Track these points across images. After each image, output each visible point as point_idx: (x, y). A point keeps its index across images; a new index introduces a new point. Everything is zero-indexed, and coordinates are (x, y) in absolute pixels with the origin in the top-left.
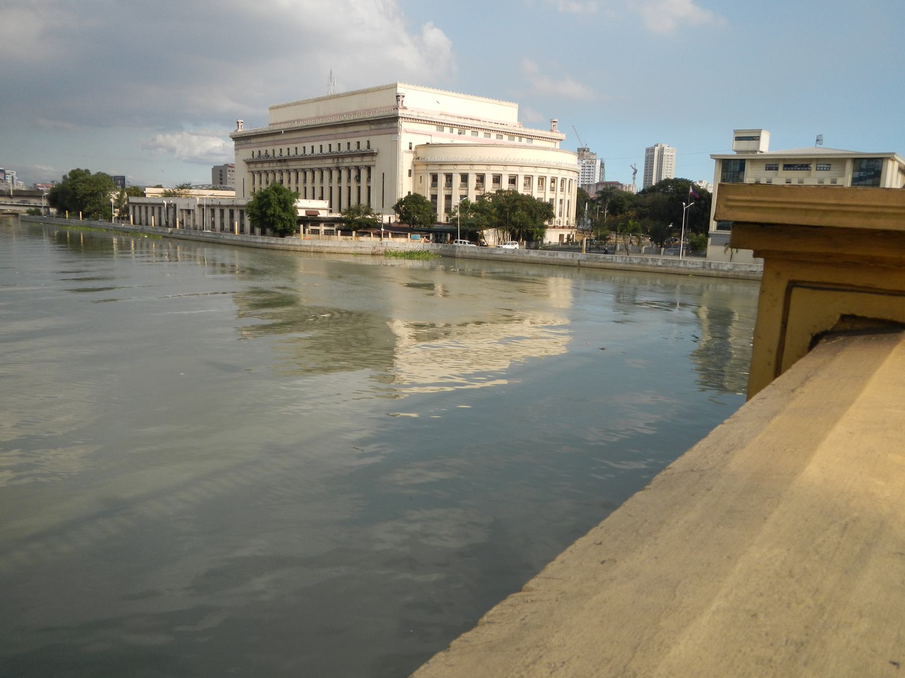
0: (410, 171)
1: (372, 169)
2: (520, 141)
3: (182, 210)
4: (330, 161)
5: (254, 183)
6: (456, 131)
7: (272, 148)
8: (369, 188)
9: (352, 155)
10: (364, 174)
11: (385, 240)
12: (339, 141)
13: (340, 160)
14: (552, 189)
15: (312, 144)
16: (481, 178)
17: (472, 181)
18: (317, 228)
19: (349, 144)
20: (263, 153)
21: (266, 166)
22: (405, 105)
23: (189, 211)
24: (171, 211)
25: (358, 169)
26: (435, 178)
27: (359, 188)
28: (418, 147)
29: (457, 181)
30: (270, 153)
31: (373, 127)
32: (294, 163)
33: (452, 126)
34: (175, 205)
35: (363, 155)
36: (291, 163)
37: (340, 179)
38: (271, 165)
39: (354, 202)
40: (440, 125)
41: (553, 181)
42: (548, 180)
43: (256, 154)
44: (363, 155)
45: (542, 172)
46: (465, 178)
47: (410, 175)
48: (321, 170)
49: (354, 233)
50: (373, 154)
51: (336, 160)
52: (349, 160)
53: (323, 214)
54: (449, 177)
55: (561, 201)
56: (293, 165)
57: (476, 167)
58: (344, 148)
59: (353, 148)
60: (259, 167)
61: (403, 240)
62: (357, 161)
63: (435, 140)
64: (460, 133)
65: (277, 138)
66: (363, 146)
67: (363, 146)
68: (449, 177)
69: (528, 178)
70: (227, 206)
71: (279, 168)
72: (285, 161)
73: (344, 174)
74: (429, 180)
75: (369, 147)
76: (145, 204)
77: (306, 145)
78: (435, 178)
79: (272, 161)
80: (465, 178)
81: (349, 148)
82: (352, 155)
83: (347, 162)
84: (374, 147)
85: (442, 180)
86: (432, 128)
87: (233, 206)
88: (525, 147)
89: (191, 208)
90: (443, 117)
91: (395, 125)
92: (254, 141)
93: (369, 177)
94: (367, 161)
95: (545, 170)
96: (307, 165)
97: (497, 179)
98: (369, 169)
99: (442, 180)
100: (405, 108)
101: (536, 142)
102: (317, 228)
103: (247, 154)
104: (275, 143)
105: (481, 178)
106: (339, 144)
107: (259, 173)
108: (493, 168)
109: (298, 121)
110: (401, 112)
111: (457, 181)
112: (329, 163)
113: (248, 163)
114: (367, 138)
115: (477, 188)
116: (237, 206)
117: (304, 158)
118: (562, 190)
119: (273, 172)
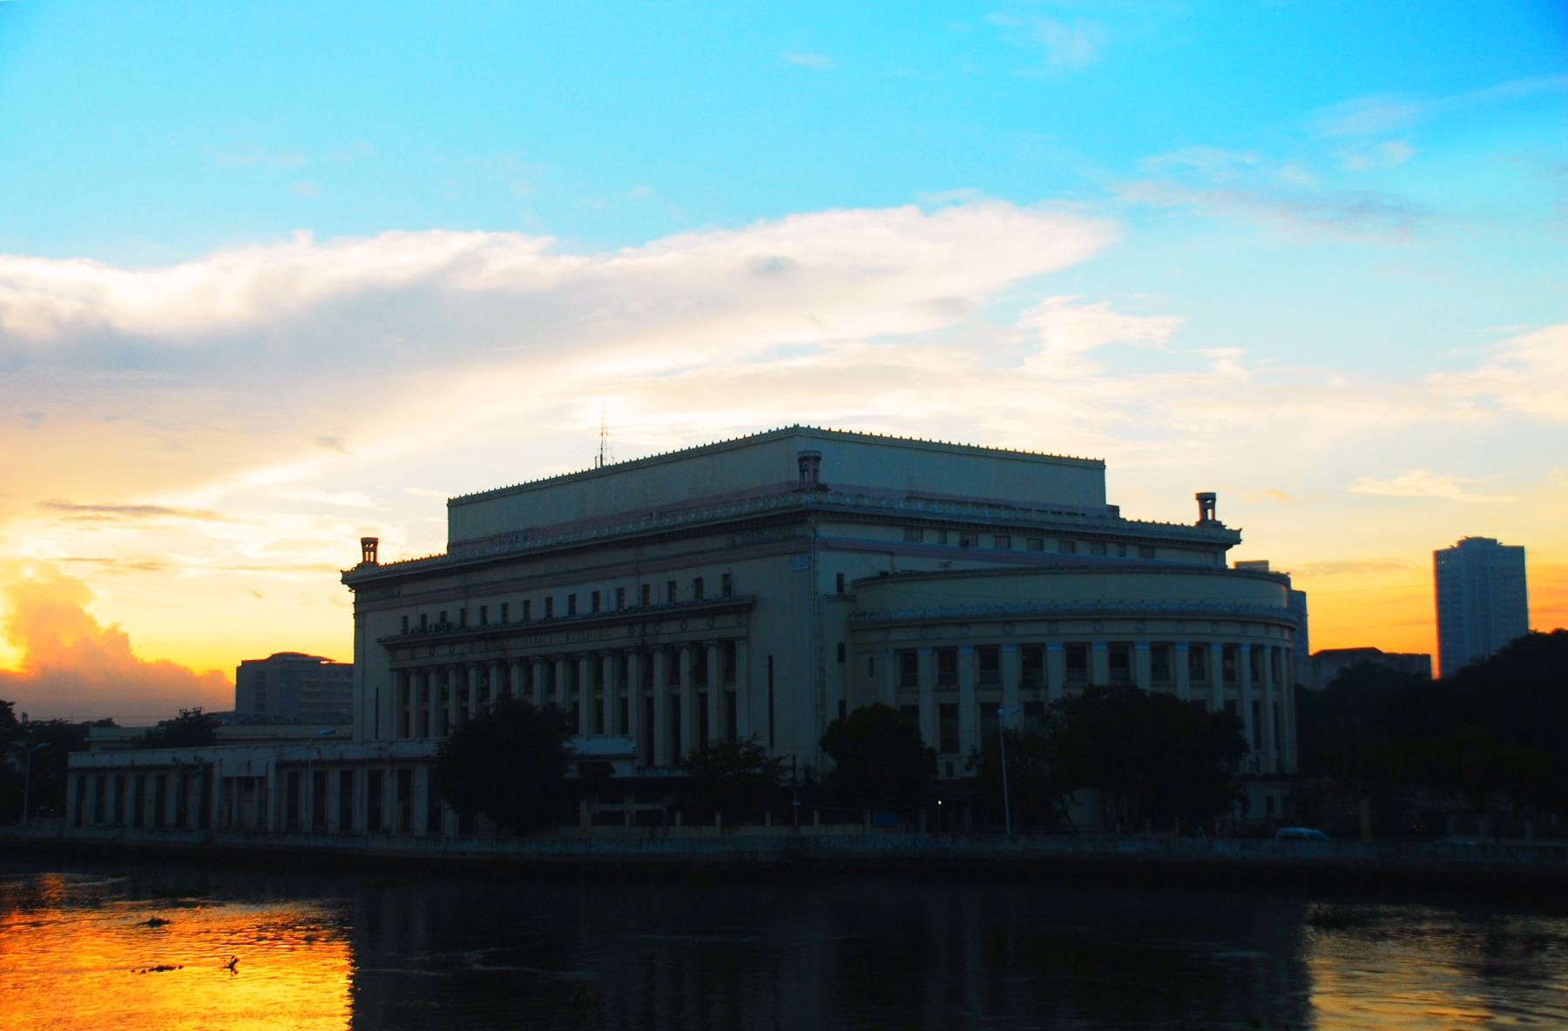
0: (841, 647)
1: (741, 650)
2: (1122, 554)
3: (227, 781)
4: (622, 631)
5: (405, 700)
6: (954, 539)
7: (461, 604)
8: (731, 698)
10: (714, 659)
11: (805, 831)
12: (645, 580)
13: (650, 628)
14: (1230, 676)
15: (571, 590)
16: (1033, 657)
17: (1011, 665)
18: (618, 807)
19: (672, 585)
20: (433, 619)
21: (443, 655)
22: (822, 479)
23: (248, 783)
24: (196, 785)
25: (699, 649)
26: (909, 661)
27: (703, 700)
28: (861, 583)
29: (968, 667)
30: (454, 617)
31: (738, 540)
33: (943, 526)
34: (208, 769)
35: (713, 612)
37: (648, 678)
38: (458, 649)
39: (715, 732)
40: (912, 524)
41: (1229, 652)
42: (1216, 654)
43: (414, 623)
44: (713, 612)
45: (1198, 631)
46: (989, 658)
47: (841, 657)
48: (596, 658)
49: (718, 818)
50: (745, 608)
51: (638, 629)
52: (674, 626)
53: (623, 771)
54: (948, 658)
55: (1256, 706)
56: (518, 648)
57: (1020, 629)
58: (658, 597)
59: (685, 594)
60: (423, 656)
61: (850, 829)
62: (697, 628)
63: (904, 564)
64: (964, 544)
65: (475, 578)
66: (713, 589)
67: (713, 589)
68: (948, 658)
69: (1160, 652)
70: (363, 762)
71: (477, 657)
73: (659, 661)
74: (890, 670)
75: (727, 588)
76: (118, 768)
77: (551, 592)
78: (909, 661)
80: (989, 658)
81: (671, 595)
82: (682, 614)
83: (670, 632)
84: (742, 588)
85: (927, 667)
86: (895, 536)
87: (379, 760)
88: (1134, 569)
89: (257, 771)
90: (920, 506)
91: (799, 531)
92: (407, 589)
93: (729, 672)
94: (725, 626)
95: (1206, 628)
96: (557, 644)
97: (1077, 657)
98: (729, 648)
99: (927, 667)
100: (823, 488)
101: (1163, 556)
102: (618, 807)
103: (389, 623)
105: (1033, 657)
106: (646, 588)
107: (423, 673)
108: (1065, 628)
109: (528, 533)
110: (809, 498)
111: (968, 667)
112: (620, 637)
113: (391, 646)
114: (722, 569)
115: (1026, 683)
116: (393, 761)
117: (550, 626)
118: (1255, 676)
119: (463, 669)
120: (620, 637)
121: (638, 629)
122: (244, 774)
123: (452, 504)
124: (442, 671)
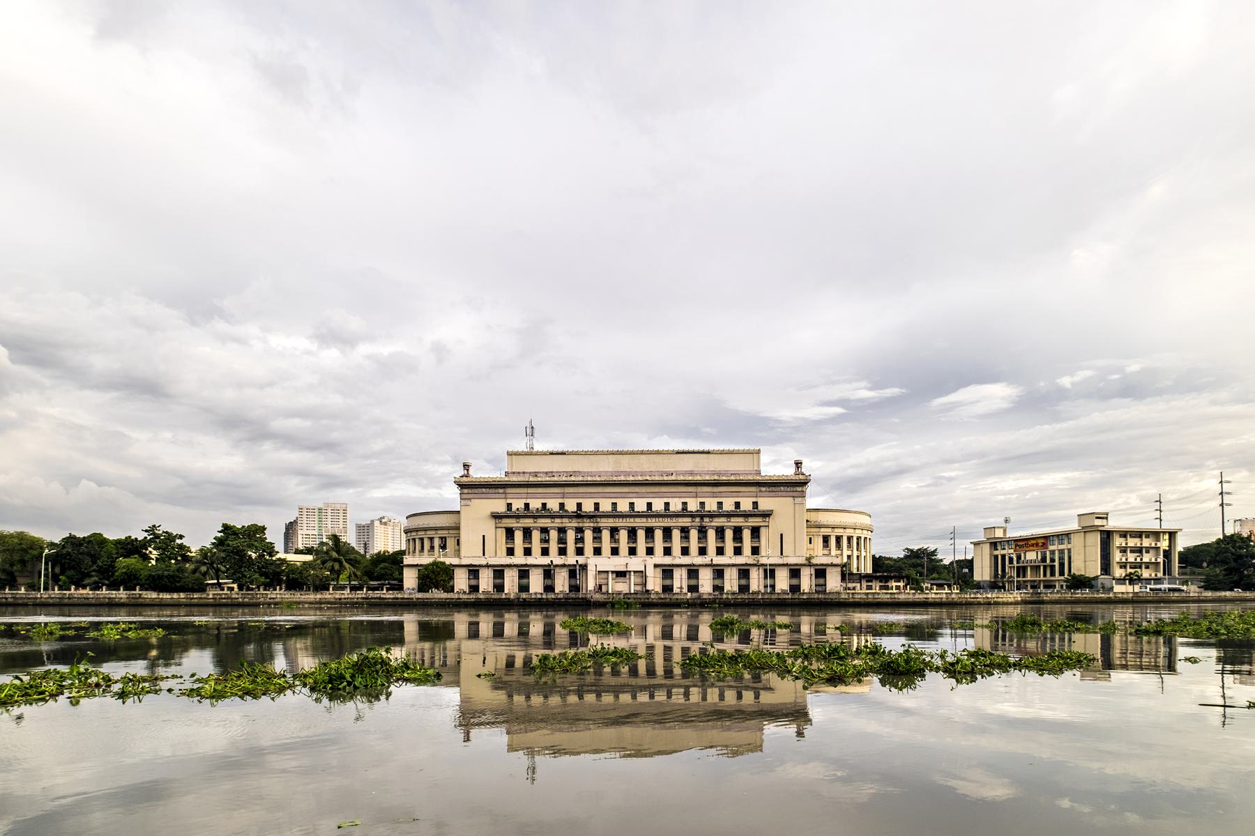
1: (763, 531)
4: (689, 519)
9: (729, 515)
13: (706, 520)
23: (621, 574)
32: (611, 520)
36: (603, 520)
38: (558, 520)
51: (698, 520)
65: (571, 490)
72: (590, 517)
79: (562, 517)
82: (729, 515)
91: (799, 489)
92: (509, 490)
94: (754, 522)
104: (564, 496)
112: (686, 522)
113: (496, 516)
120: (686, 522)
121: (698, 520)
122: (623, 569)
123: (510, 454)
124: (545, 530)
